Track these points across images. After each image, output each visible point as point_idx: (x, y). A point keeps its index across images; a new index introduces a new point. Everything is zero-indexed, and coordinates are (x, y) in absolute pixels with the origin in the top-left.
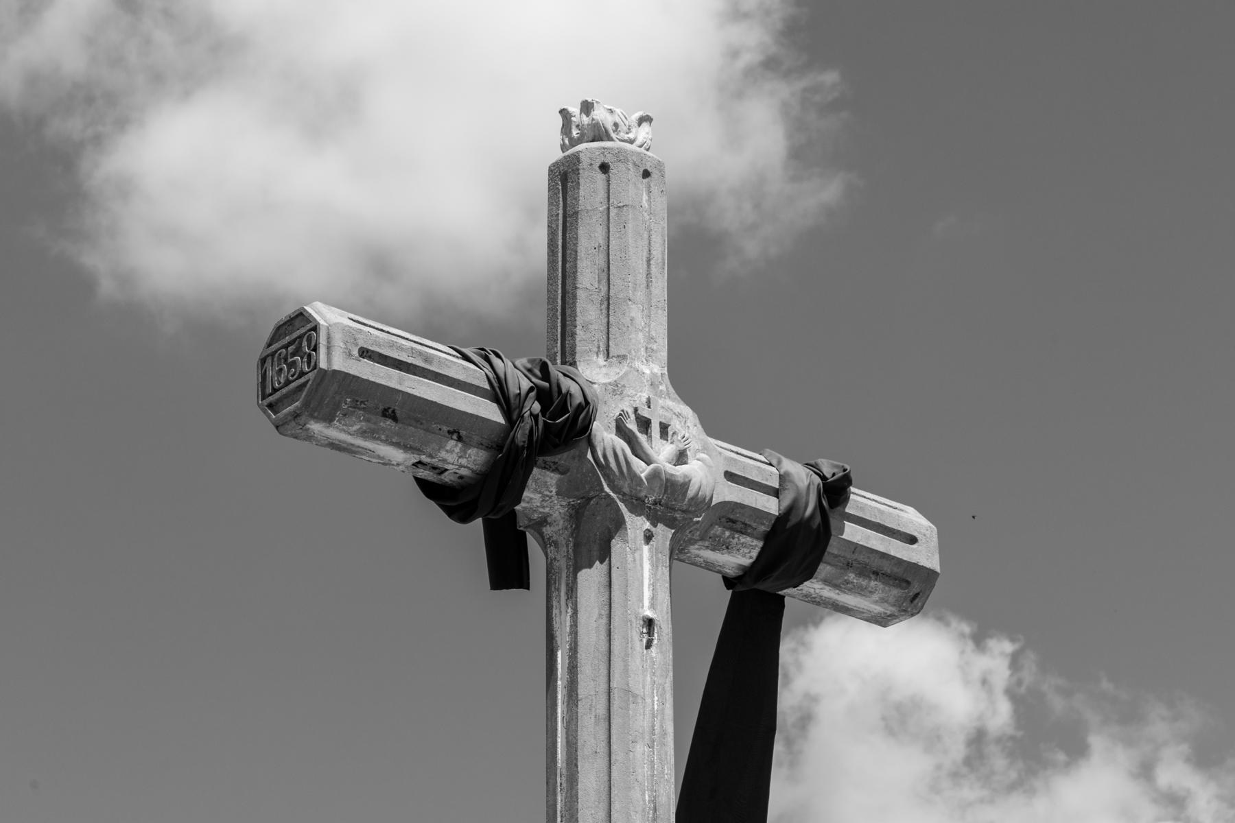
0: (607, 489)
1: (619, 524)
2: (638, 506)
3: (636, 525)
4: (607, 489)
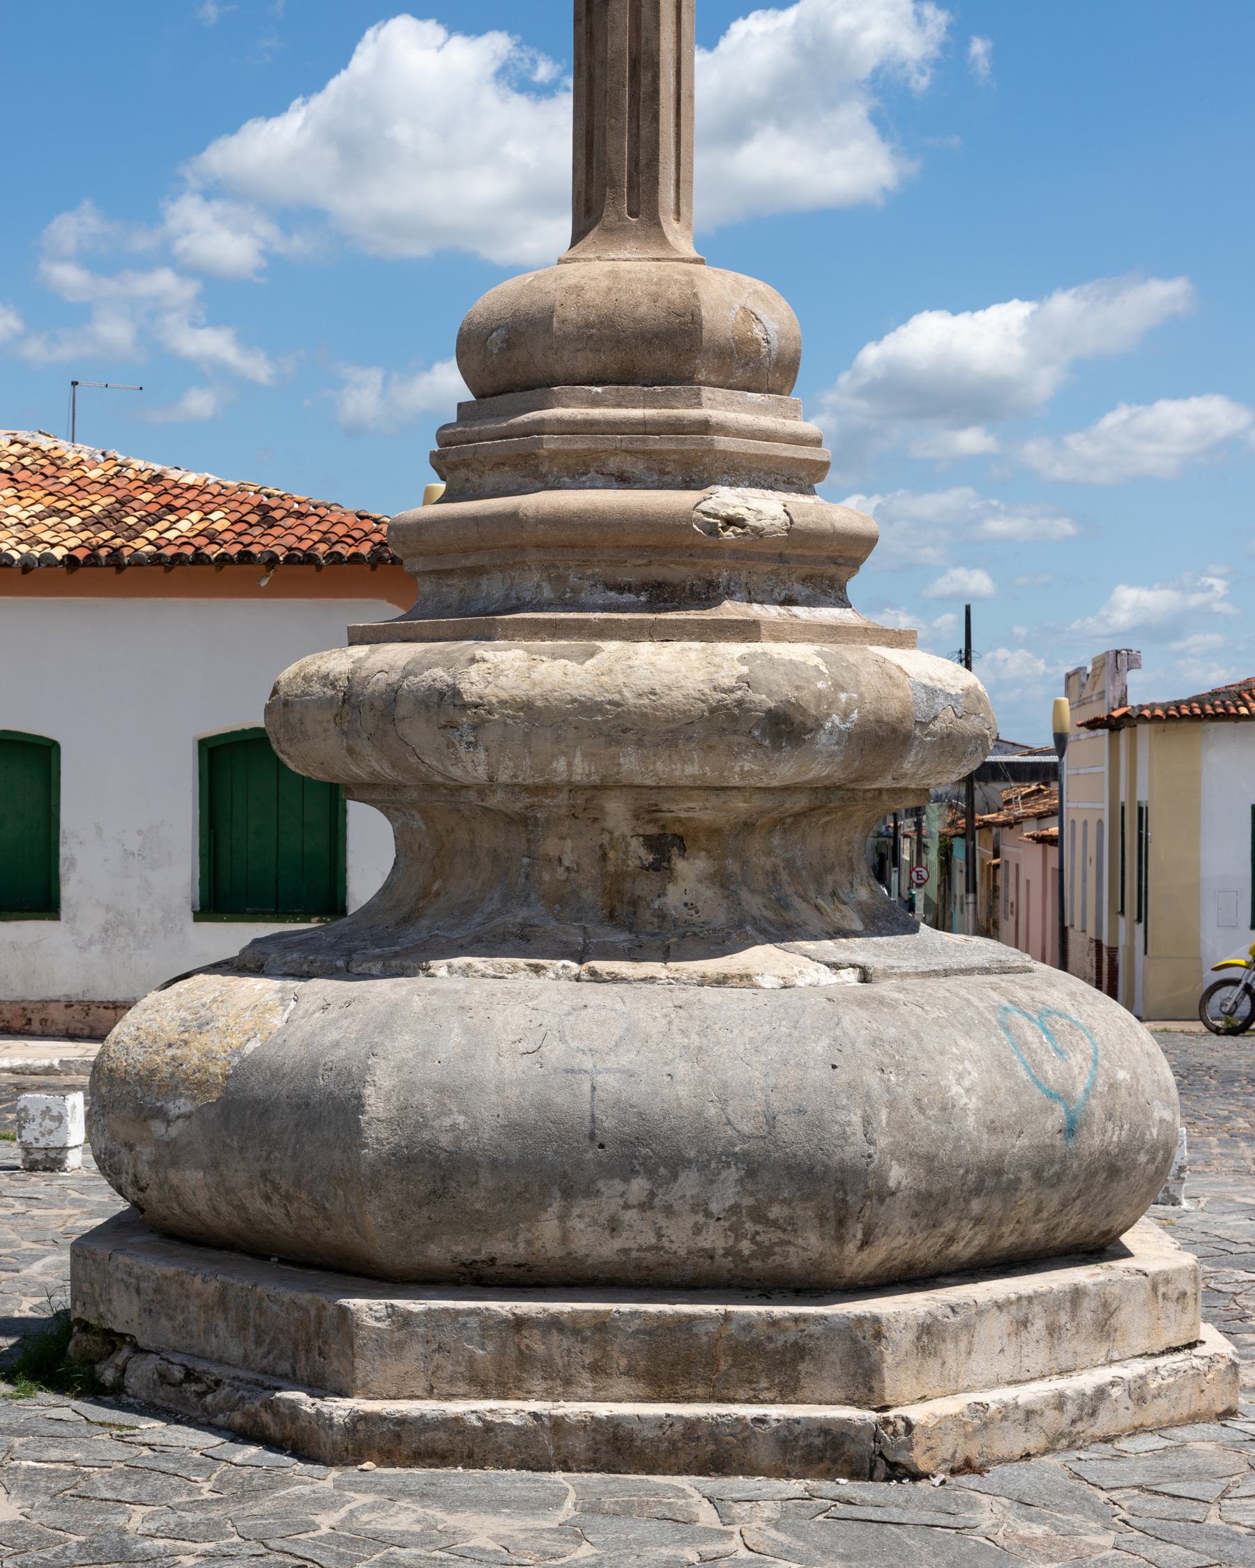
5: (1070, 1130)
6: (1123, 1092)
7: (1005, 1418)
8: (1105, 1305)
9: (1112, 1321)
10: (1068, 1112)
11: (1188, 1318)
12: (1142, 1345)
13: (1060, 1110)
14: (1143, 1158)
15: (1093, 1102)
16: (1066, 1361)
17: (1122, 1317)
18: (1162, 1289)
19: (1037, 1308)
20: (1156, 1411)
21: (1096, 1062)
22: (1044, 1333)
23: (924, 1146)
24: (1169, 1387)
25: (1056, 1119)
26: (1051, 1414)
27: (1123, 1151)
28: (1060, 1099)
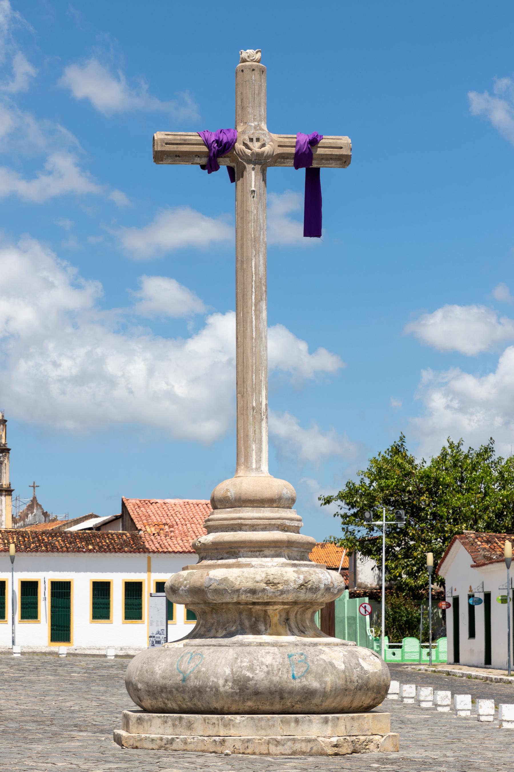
0: (240, 160)
1: (245, 168)
2: (249, 162)
3: (249, 167)
4: (240, 160)
5: (184, 680)
6: (202, 673)
8: (189, 722)
9: (192, 726)
10: (183, 676)
11: (216, 729)
12: (201, 733)
13: (181, 675)
14: (208, 690)
15: (192, 675)
16: (179, 733)
17: (195, 725)
18: (207, 721)
20: (189, 747)
21: (197, 666)
22: (171, 725)
23: (146, 680)
24: (194, 742)
25: (181, 677)
27: (201, 687)
28: (182, 673)
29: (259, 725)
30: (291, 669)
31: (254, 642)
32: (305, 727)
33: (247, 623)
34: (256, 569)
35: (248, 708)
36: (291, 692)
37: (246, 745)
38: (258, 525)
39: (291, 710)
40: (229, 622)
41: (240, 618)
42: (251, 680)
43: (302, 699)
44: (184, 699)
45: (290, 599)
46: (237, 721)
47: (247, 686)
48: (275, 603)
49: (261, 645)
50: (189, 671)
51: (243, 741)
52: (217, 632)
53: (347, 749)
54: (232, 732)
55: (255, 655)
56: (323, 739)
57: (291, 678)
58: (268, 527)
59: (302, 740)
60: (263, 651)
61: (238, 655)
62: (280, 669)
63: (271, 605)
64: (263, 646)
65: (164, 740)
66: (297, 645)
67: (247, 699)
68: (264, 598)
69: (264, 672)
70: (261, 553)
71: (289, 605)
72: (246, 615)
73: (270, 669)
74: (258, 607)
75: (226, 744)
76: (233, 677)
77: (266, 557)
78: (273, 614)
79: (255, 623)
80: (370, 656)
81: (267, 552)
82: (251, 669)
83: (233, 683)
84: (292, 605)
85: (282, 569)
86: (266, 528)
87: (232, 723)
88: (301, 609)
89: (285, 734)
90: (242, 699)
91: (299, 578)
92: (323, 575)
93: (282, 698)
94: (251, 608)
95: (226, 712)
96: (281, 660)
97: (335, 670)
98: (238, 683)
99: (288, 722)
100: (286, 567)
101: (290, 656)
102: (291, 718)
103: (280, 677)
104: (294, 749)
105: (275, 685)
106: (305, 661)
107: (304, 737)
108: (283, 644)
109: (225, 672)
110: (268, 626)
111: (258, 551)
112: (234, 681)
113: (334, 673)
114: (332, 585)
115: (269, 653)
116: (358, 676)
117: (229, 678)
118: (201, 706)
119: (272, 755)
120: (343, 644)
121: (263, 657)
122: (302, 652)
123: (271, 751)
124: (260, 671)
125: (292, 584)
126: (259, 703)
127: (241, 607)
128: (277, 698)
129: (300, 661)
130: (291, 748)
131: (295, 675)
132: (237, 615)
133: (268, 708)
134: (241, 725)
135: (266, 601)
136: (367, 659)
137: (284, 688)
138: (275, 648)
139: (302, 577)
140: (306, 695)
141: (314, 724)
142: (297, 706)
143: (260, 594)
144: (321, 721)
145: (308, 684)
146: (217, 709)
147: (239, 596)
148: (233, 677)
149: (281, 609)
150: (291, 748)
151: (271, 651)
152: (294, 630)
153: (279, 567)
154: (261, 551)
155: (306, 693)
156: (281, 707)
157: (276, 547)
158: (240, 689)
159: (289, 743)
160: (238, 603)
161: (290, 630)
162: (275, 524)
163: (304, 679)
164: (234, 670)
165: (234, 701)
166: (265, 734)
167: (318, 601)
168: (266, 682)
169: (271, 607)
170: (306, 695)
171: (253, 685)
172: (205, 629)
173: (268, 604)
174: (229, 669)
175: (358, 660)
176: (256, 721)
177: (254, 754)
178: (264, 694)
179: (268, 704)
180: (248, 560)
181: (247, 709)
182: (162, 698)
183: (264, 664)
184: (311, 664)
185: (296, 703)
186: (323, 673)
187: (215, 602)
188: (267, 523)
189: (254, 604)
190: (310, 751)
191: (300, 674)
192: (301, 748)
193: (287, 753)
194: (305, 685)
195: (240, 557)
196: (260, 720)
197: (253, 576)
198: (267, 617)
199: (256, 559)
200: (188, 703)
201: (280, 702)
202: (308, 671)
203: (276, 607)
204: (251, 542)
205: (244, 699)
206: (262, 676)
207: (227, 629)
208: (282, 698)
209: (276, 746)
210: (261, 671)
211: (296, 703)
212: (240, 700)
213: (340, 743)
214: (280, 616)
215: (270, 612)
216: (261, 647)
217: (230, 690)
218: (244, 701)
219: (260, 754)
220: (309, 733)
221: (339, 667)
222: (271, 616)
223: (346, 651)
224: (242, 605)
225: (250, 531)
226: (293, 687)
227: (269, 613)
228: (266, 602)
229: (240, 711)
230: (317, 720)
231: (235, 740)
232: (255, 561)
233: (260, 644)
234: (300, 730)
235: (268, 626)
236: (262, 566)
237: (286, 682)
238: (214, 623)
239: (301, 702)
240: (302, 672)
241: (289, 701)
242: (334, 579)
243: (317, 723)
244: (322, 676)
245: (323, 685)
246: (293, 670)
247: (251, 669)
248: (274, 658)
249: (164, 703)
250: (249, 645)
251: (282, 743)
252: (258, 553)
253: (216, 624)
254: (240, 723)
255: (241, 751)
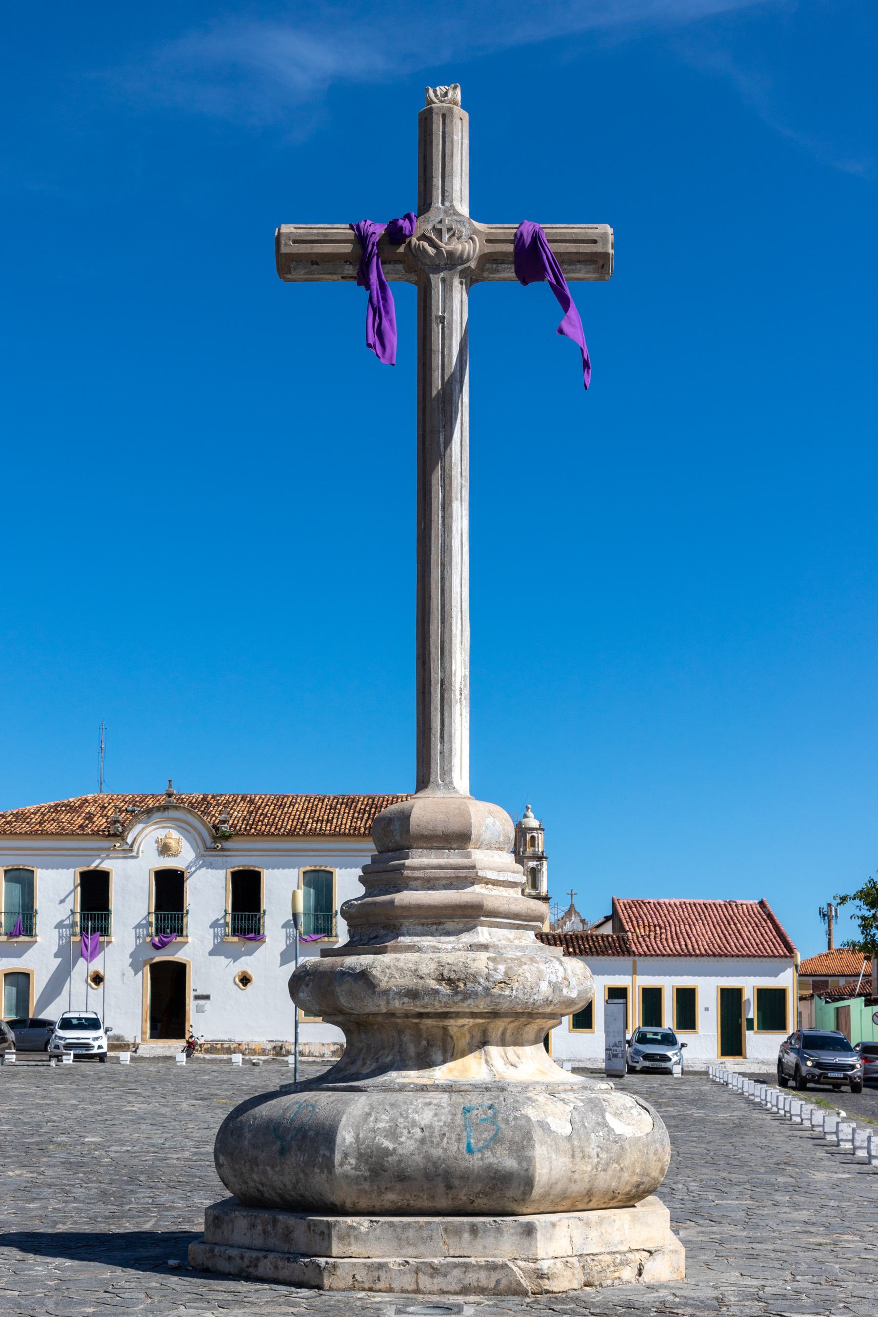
7: (220, 1256)
8: (287, 1228)
13: (279, 1143)
18: (312, 1228)
19: (258, 1221)
26: (238, 1261)
29: (404, 1237)
30: (465, 1134)
31: (410, 1084)
32: (490, 1241)
33: (412, 1050)
34: (423, 955)
35: (389, 1204)
36: (465, 1176)
37: (376, 1274)
38: (438, 879)
39: (470, 1208)
40: (384, 1048)
41: (400, 1040)
42: (392, 1155)
43: (487, 1190)
44: (285, 1186)
45: (482, 1007)
46: (363, 1229)
47: (383, 1166)
48: (458, 1015)
49: (423, 1090)
50: (290, 1136)
51: (369, 1267)
52: (364, 1064)
53: (570, 1281)
54: (354, 1249)
55: (404, 1107)
56: (520, 1263)
57: (465, 1152)
58: (455, 883)
59: (481, 1267)
60: (419, 1100)
61: (372, 1108)
62: (444, 1134)
63: (451, 1018)
64: (427, 1090)
65: (245, 1260)
66: (487, 1089)
67: (386, 1189)
68: (434, 1005)
69: (416, 1140)
70: (441, 927)
71: (484, 1018)
72: (411, 1035)
73: (427, 1134)
74: (429, 1022)
75: (339, 1272)
76: (359, 1149)
77: (448, 934)
78: (459, 1034)
79: (426, 1049)
80: (632, 1108)
81: (450, 925)
82: (391, 1133)
83: (357, 1159)
84: (489, 1018)
85: (471, 955)
86: (451, 884)
87: (353, 1233)
88: (512, 1025)
89: (452, 1253)
90: (375, 1187)
91: (495, 970)
92: (547, 965)
93: (449, 1187)
94: (416, 1023)
95: (351, 1210)
96: (450, 1117)
97: (549, 1136)
98: (367, 1160)
99: (456, 1232)
100: (477, 950)
101: (466, 1110)
102: (463, 1223)
103: (445, 1150)
104: (466, 1282)
105: (435, 1164)
106: (493, 1120)
107: (482, 1261)
108: (463, 1088)
109: (345, 1139)
110: (449, 1054)
111: (435, 924)
112: (360, 1156)
113: (546, 1142)
114: (566, 983)
115: (430, 1104)
116: (598, 1146)
117: (350, 1151)
118: (310, 1199)
119: (424, 1293)
120: (585, 1088)
121: (417, 1112)
122: (490, 1102)
123: (421, 1286)
124: (408, 1138)
125: (482, 981)
126: (408, 1197)
127: (398, 1021)
128: (441, 1188)
129: (484, 1120)
130: (460, 1281)
131: (473, 1146)
132: (395, 1034)
133: (426, 1204)
134: (371, 1236)
135: (440, 1011)
136: (624, 1115)
137: (453, 1169)
138: (446, 1096)
139: (502, 968)
140: (494, 1182)
141: (506, 1236)
142: (479, 1200)
143: (426, 999)
144: (519, 1230)
145: (496, 1162)
146: (335, 1205)
147: (388, 1003)
148: (359, 1149)
149: (471, 1025)
150: (460, 1281)
151: (435, 1101)
152: (494, 1063)
153: (466, 951)
154: (440, 923)
155: (494, 1178)
156: (450, 1202)
157: (465, 917)
158: (370, 1170)
159: (456, 1272)
160: (392, 1015)
161: (487, 1061)
162: (466, 878)
163: (488, 1154)
164: (360, 1136)
165: (362, 1191)
166: (414, 1254)
167: (541, 1010)
168: (418, 1159)
169: (452, 1022)
170: (494, 1182)
171: (395, 1164)
172: (348, 1060)
173: (445, 1015)
174: (352, 1134)
175: (604, 1117)
176: (398, 1230)
177: (390, 1290)
178: (415, 1179)
179: (425, 1197)
180: (416, 939)
181: (387, 1205)
182: (254, 1181)
183: (416, 1126)
184: (503, 1126)
185: (477, 1195)
186: (525, 1143)
187: (355, 1012)
188: (453, 875)
189: (420, 1015)
190: (496, 1286)
191: (481, 1144)
192: (478, 1280)
193: (452, 1291)
194: (491, 1164)
195: (403, 935)
196: (405, 1227)
197: (414, 967)
198: (449, 1039)
199: (429, 938)
200: (292, 1193)
201: (447, 1194)
202: (497, 1139)
203: (461, 1022)
204: (419, 907)
205: (379, 1188)
206: (412, 1148)
207: (380, 1060)
208: (449, 1187)
209: (432, 1276)
210: (411, 1138)
211: (477, 1195)
212: (372, 1191)
213: (555, 1270)
214: (472, 1037)
215: (453, 1031)
216: (420, 1094)
217: (353, 1172)
218: (380, 1193)
219: (403, 1291)
220: (496, 1252)
221: (559, 1131)
222: (455, 1038)
223: (582, 1101)
224: (399, 1018)
225: (423, 889)
226: (468, 1167)
227: (451, 1033)
228: (443, 1013)
229: (377, 1209)
230: (514, 1228)
231: (354, 1264)
232: (427, 941)
233: (424, 1088)
234: (480, 1248)
235: (449, 1054)
236: (435, 950)
237: (456, 1159)
238: (362, 1049)
239: (486, 1195)
240: (486, 1141)
241: (464, 1192)
242: (569, 972)
243: (512, 1235)
244: (523, 1147)
245: (524, 1164)
246: (469, 1137)
247: (392, 1133)
248: (436, 1115)
249: (258, 1190)
250: (402, 1088)
251: (443, 1270)
252: (435, 927)
253: (364, 1051)
254: (368, 1233)
255: (366, 1286)
